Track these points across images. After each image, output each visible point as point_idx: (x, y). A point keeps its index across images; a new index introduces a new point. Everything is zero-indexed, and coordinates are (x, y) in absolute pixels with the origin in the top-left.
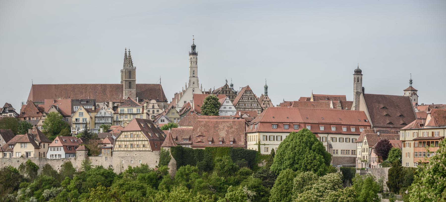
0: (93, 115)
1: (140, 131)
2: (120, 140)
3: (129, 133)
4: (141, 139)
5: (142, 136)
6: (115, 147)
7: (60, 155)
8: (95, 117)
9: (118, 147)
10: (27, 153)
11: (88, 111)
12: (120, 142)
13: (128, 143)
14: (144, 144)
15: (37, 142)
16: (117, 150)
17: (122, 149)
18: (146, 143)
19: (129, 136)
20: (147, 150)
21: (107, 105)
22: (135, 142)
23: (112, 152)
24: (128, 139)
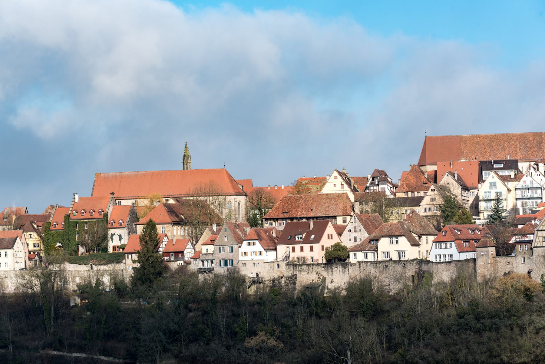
0: (512, 185)
6: (537, 240)
7: (451, 256)
8: (516, 189)
9: (541, 241)
10: (399, 254)
11: (505, 179)
16: (539, 245)
21: (535, 169)
23: (531, 249)
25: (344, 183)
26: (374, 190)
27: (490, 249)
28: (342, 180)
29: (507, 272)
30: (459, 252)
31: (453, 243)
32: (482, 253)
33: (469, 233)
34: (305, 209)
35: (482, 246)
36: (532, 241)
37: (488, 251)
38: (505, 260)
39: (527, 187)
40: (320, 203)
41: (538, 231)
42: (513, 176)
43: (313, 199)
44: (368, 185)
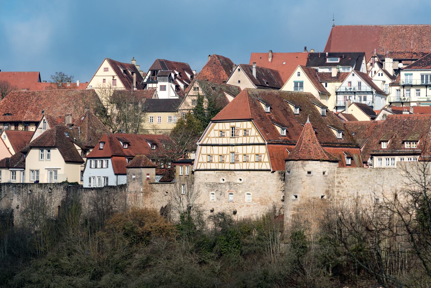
1: (250, 120)
2: (209, 142)
3: (227, 126)
4: (251, 142)
5: (253, 131)
6: (201, 160)
12: (209, 147)
13: (225, 148)
14: (257, 152)
15: (77, 147)
17: (213, 166)
18: (263, 149)
19: (228, 134)
20: (264, 167)
22: (239, 149)
23: (193, 172)
24: (225, 141)
25: (117, 78)
26: (152, 88)
27: (144, 171)
28: (114, 74)
29: (164, 207)
30: (116, 174)
31: (110, 160)
32: (134, 177)
33: (147, 147)
34: (35, 111)
35: (134, 166)
36: (194, 160)
37: (141, 174)
38: (163, 188)
39: (352, 90)
40: (56, 103)
41: (202, 145)
42: (334, 74)
43: (48, 97)
44: (145, 81)
